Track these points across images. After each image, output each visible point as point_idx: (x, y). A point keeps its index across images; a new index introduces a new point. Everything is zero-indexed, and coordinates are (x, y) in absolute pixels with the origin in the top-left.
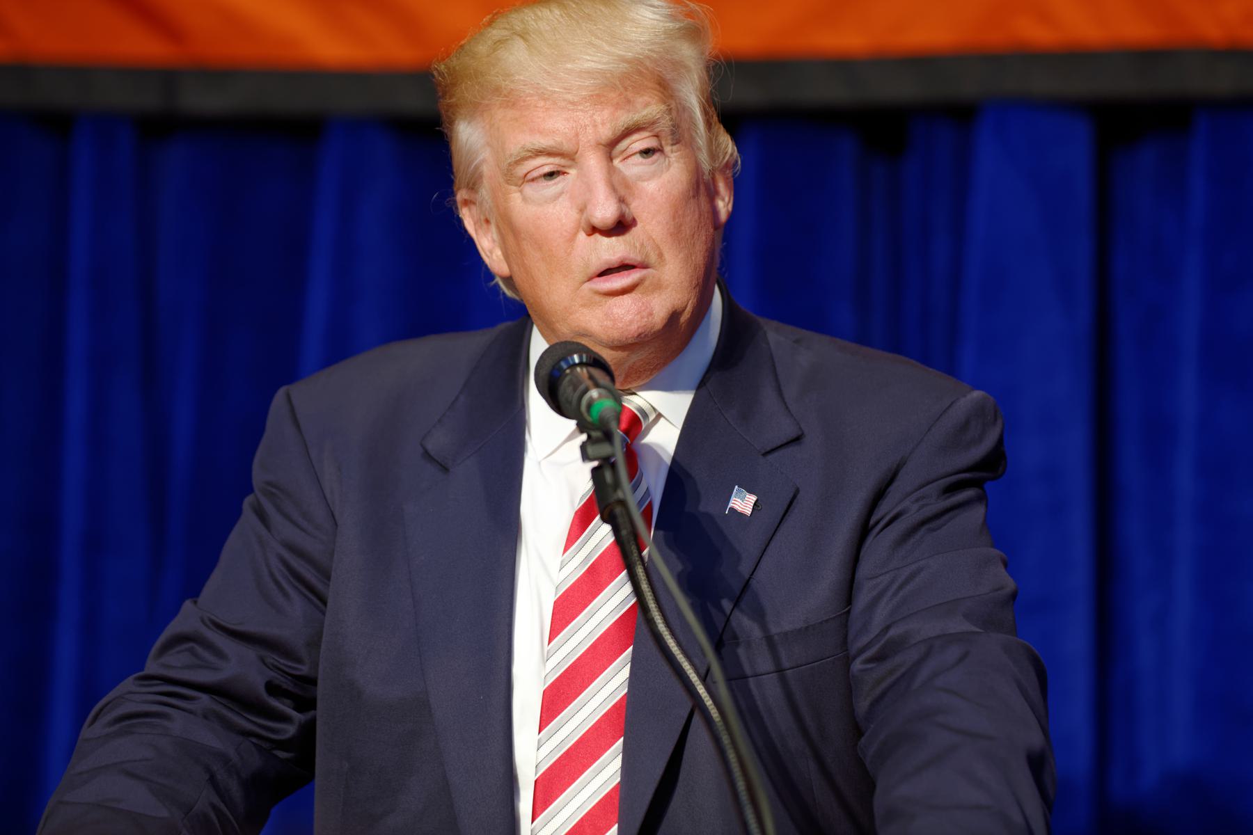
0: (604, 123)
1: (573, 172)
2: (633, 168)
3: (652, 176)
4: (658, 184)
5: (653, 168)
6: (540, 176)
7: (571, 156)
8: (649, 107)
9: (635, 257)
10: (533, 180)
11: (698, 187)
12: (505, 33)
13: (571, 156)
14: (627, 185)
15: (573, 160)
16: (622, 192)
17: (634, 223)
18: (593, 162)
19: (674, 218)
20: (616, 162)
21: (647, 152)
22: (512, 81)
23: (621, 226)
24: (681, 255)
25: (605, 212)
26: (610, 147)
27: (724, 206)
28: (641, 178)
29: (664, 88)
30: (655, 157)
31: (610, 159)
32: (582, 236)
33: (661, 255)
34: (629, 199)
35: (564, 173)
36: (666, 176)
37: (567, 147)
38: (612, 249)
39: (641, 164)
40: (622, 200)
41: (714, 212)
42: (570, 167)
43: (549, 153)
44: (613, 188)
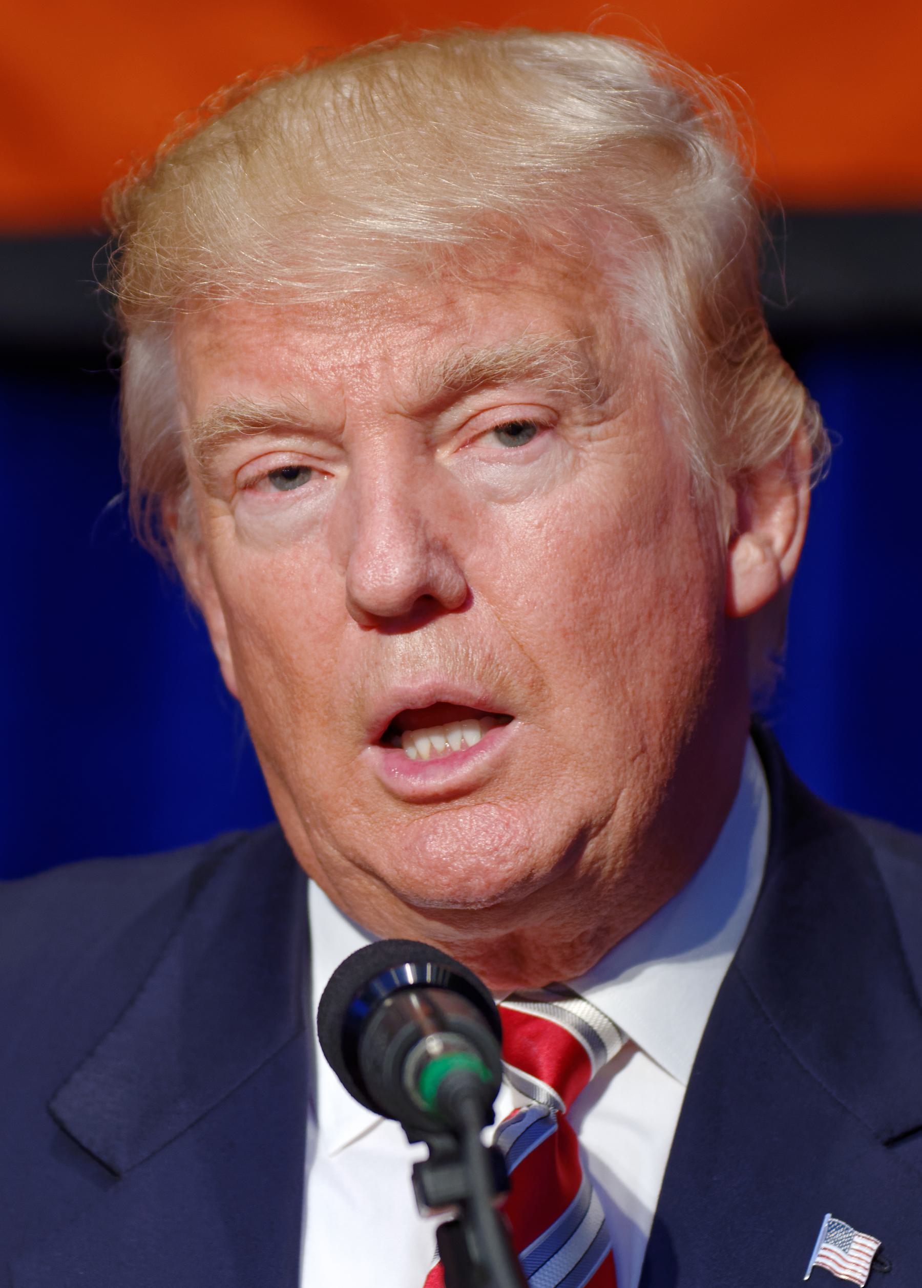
0: (412, 359)
1: (341, 471)
2: (490, 467)
3: (527, 491)
4: (535, 517)
5: (526, 472)
6: (261, 477)
7: (335, 438)
8: (519, 328)
9: (468, 687)
10: (251, 486)
11: (662, 517)
12: (228, 134)
13: (335, 438)
14: (458, 511)
15: (340, 446)
16: (441, 527)
17: (464, 602)
18: (380, 454)
19: (576, 594)
20: (444, 455)
21: (515, 432)
22: (195, 255)
23: (423, 607)
24: (594, 683)
25: (389, 571)
26: (429, 416)
27: (758, 565)
28: (494, 495)
29: (581, 279)
30: (538, 443)
31: (430, 447)
32: (353, 630)
33: (538, 686)
34: (459, 545)
35: (325, 473)
36: (562, 495)
37: (316, 415)
38: (418, 662)
39: (500, 460)
40: (434, 547)
41: (721, 578)
42: (335, 460)
43: (279, 430)
44: (412, 518)
